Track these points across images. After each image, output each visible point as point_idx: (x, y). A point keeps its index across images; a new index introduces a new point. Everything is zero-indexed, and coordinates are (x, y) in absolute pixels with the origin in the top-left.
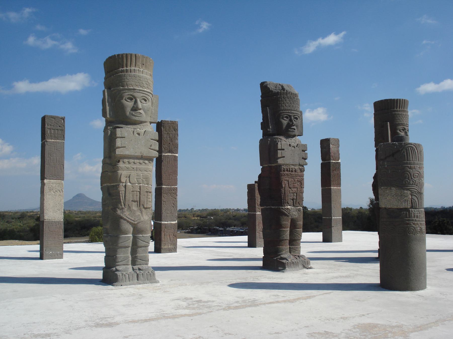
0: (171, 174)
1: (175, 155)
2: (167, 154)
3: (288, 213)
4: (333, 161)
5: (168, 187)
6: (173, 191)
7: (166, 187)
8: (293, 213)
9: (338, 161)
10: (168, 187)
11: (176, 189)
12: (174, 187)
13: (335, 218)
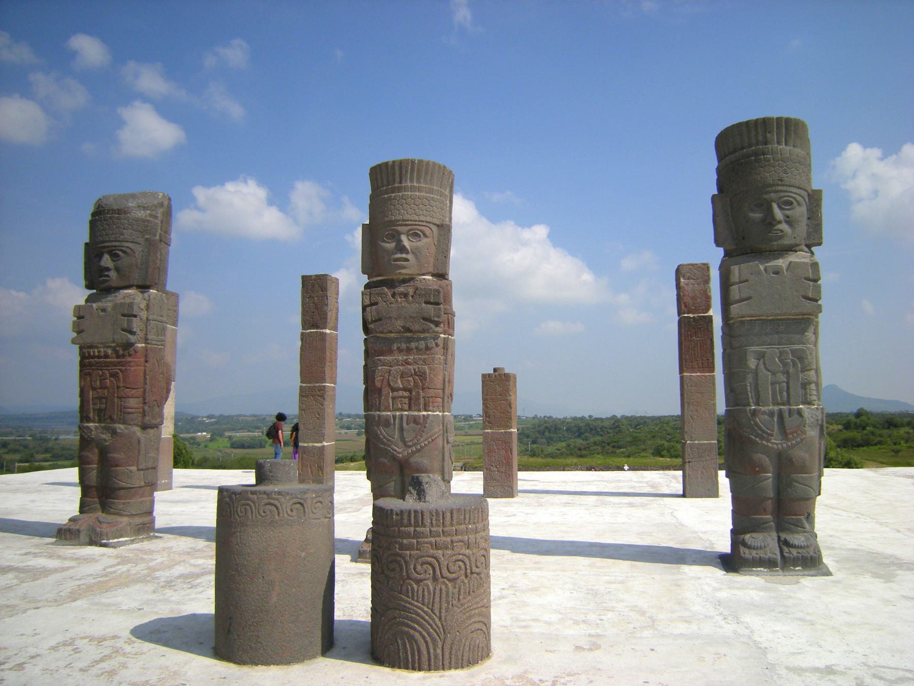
0: (315, 362)
1: (321, 331)
2: (309, 331)
3: (89, 436)
4: (689, 315)
6: (318, 392)
8: (101, 435)
9: (706, 313)
11: (323, 388)
12: (321, 385)
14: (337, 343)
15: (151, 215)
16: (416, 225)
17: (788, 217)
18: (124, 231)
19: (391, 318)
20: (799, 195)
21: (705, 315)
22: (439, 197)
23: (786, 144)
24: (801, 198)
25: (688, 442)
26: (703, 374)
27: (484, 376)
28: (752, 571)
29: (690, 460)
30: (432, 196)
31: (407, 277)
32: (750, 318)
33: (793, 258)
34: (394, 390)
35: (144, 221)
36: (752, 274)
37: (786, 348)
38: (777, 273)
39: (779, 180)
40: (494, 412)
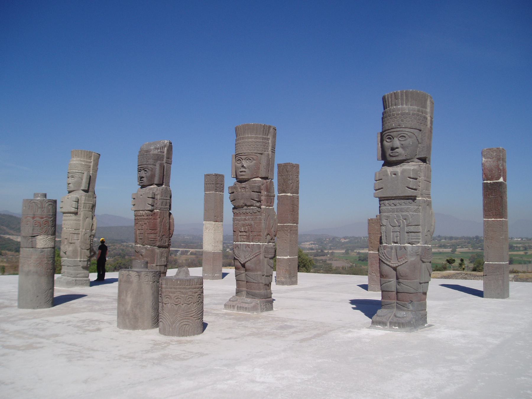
1: (287, 194)
4: (487, 182)
5: (281, 224)
7: (280, 224)
9: (499, 180)
10: (281, 224)
13: (491, 263)
14: (298, 201)
15: (161, 152)
16: (249, 155)
17: (402, 145)
18: (148, 160)
19: (239, 199)
21: (498, 181)
22: (262, 140)
23: (406, 105)
25: (486, 263)
26: (496, 219)
28: (375, 327)
29: (487, 274)
30: (257, 140)
31: (247, 179)
33: (406, 166)
34: (240, 232)
35: (157, 155)
36: (384, 176)
37: (399, 214)
38: (395, 174)
39: (399, 125)
40: (374, 241)
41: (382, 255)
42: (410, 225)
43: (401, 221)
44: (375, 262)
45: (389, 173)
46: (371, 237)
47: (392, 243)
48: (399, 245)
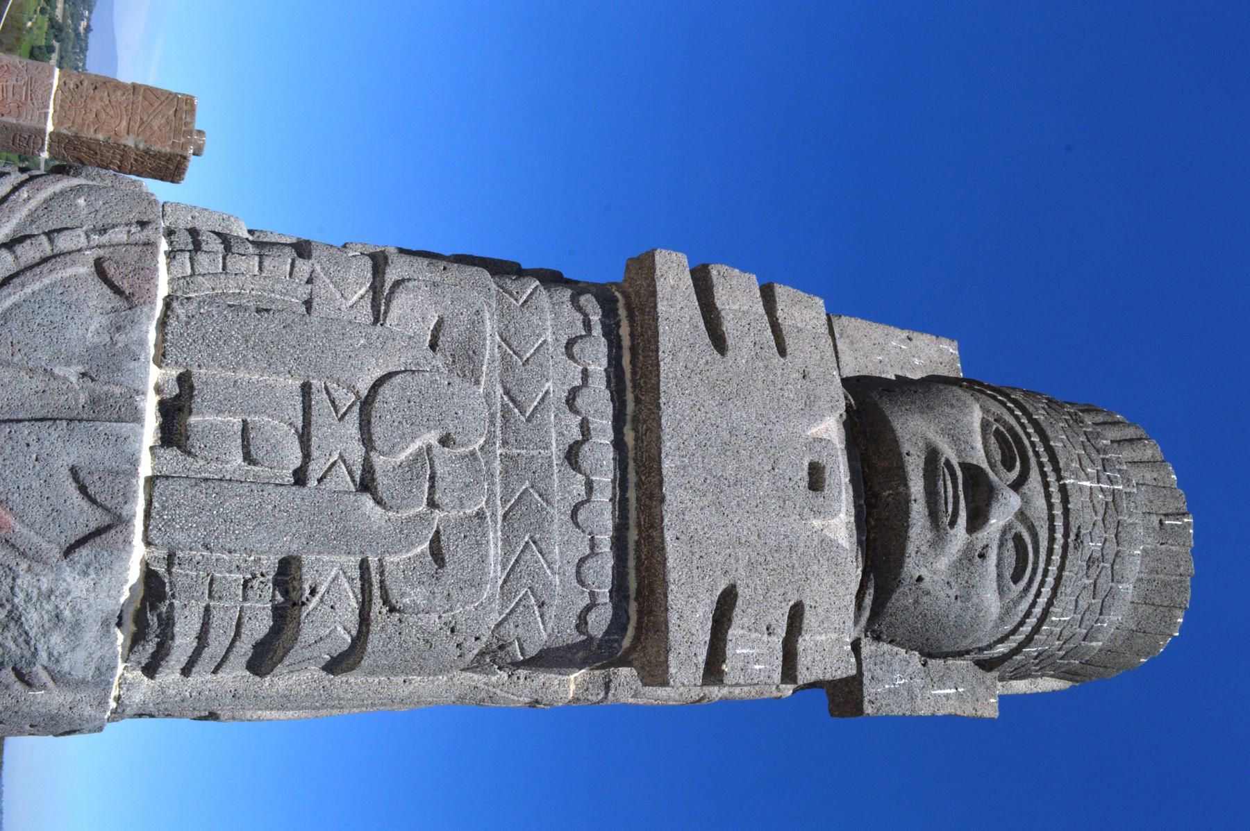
17: (982, 556)
20: (1028, 614)
24: (1021, 615)
27: (189, 101)
32: (626, 342)
37: (491, 493)
40: (101, 99)
41: (32, 218)
42: (377, 605)
43: (423, 508)
44: (12, 83)
45: (815, 430)
46: (119, 93)
47: (174, 373)
48: (146, 468)
